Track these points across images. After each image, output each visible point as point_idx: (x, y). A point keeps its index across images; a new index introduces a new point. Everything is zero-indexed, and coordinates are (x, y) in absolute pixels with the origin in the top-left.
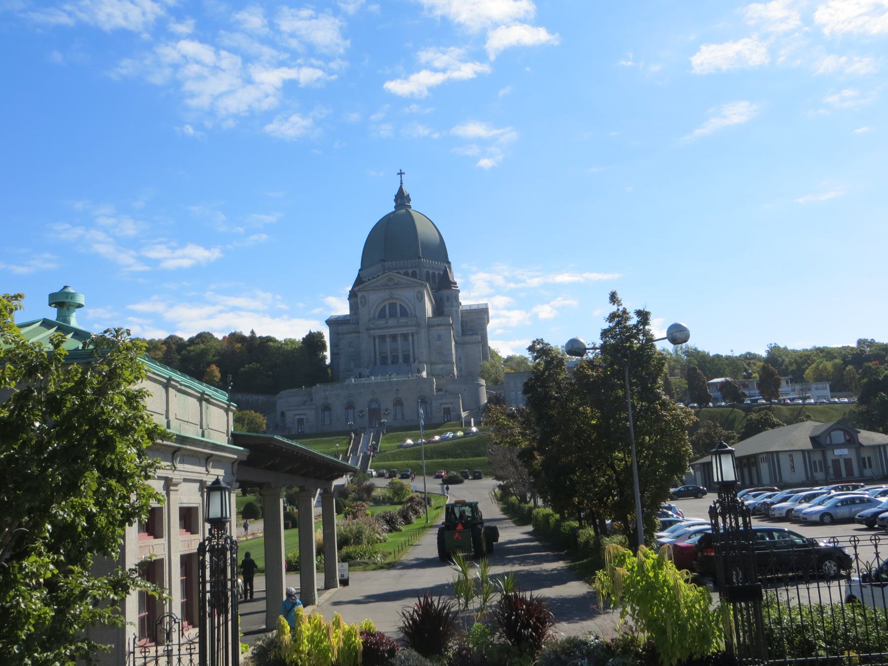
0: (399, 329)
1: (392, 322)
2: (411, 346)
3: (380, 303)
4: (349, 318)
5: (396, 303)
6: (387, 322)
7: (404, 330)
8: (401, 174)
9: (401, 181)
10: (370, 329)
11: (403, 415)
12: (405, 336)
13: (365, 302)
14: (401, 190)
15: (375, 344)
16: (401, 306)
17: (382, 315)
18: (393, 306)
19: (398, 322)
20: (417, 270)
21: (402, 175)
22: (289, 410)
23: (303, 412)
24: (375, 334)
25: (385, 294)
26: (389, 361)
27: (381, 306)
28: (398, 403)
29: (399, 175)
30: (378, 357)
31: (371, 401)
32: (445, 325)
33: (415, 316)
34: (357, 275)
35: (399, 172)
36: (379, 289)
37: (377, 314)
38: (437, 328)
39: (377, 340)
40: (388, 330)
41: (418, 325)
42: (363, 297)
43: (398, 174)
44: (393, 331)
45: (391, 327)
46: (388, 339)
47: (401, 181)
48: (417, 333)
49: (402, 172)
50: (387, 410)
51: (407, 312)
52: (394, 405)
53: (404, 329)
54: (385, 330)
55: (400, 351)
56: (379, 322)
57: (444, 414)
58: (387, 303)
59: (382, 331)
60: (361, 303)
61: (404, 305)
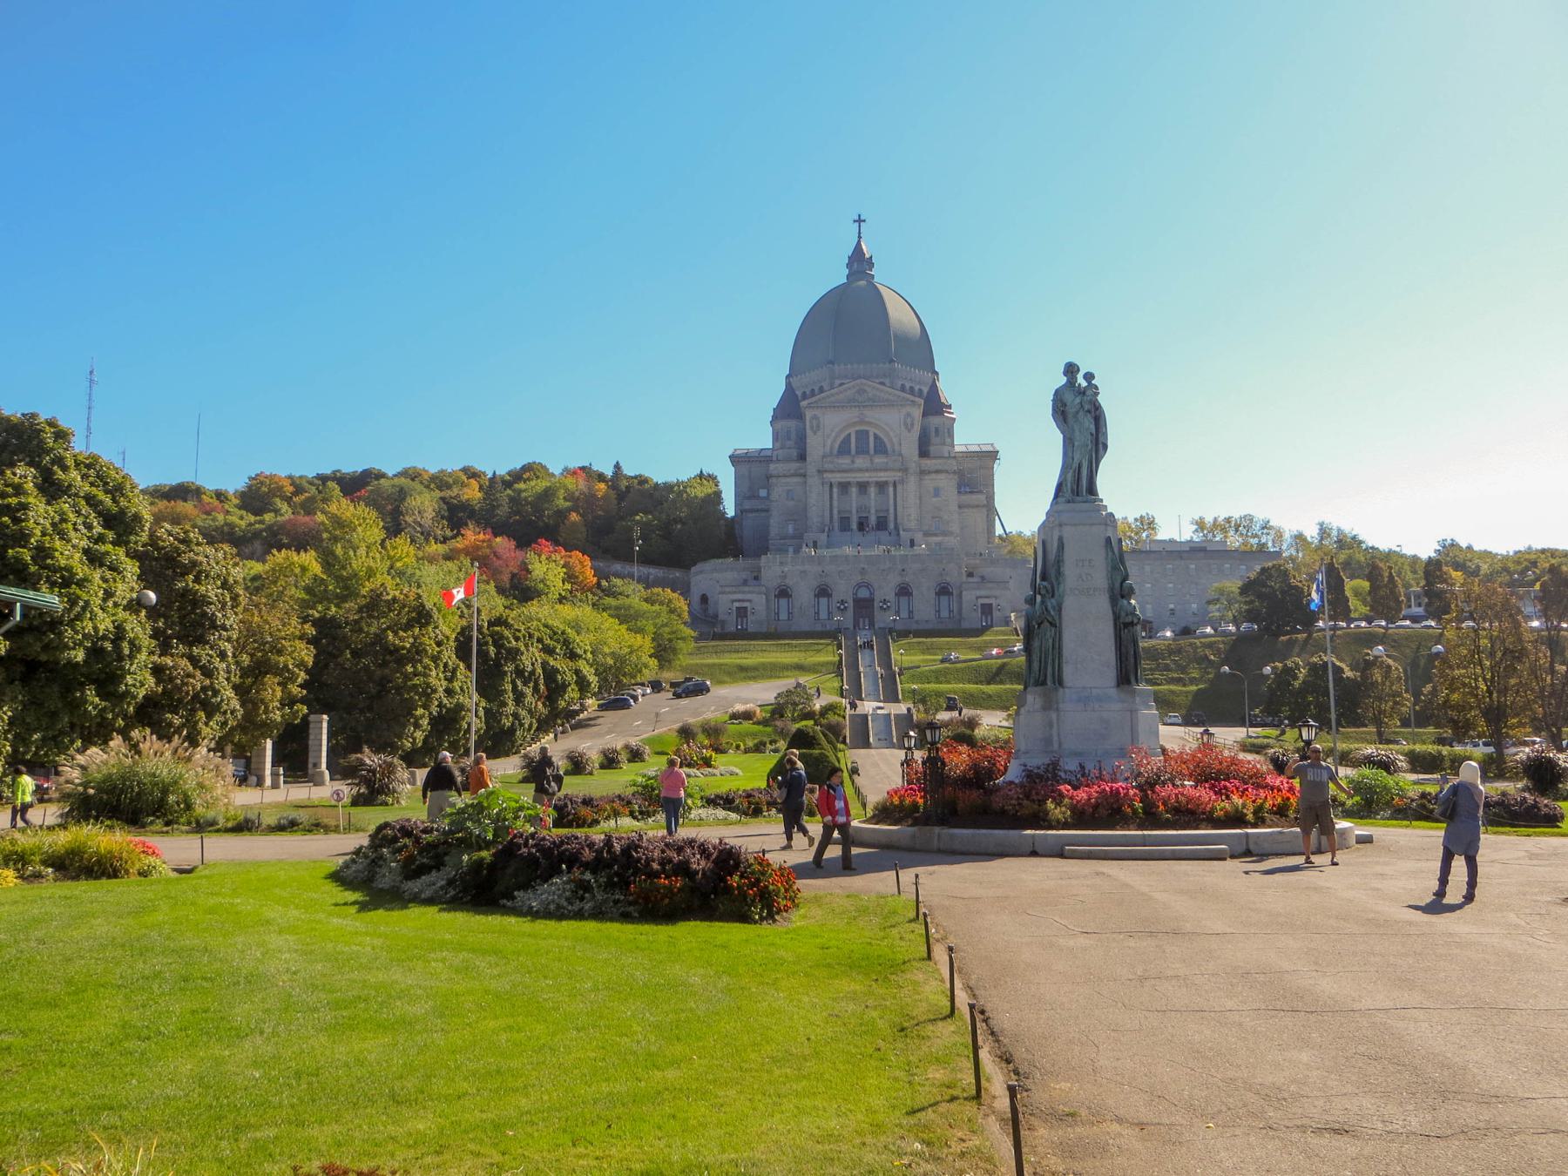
1: (861, 462)
2: (891, 501)
3: (841, 431)
4: (769, 453)
5: (867, 432)
6: (853, 462)
7: (883, 476)
8: (860, 221)
9: (859, 233)
10: (826, 471)
11: (910, 612)
12: (882, 486)
13: (818, 426)
14: (858, 249)
15: (831, 497)
16: (876, 437)
17: (844, 449)
18: (862, 435)
19: (872, 463)
20: (887, 381)
22: (723, 593)
23: (748, 596)
24: (833, 480)
26: (854, 526)
27: (842, 436)
28: (904, 591)
29: (857, 224)
30: (836, 516)
31: (859, 586)
32: (947, 472)
33: (900, 455)
34: (781, 388)
35: (857, 218)
37: (837, 446)
38: (933, 476)
39: (835, 490)
40: (853, 475)
41: (905, 470)
42: (815, 417)
45: (860, 470)
47: (859, 233)
48: (902, 481)
49: (862, 218)
50: (885, 602)
51: (885, 446)
52: (896, 594)
53: (882, 474)
55: (873, 511)
56: (840, 461)
57: (983, 613)
58: (852, 431)
59: (845, 475)
60: (812, 427)
61: (881, 435)
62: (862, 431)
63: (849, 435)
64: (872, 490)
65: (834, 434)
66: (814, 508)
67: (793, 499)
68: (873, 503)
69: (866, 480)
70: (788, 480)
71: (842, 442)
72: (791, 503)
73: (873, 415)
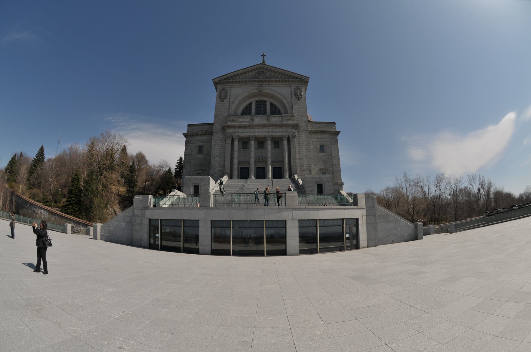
0: (270, 130)
5: (265, 102)
6: (252, 120)
7: (278, 132)
8: (263, 56)
13: (226, 96)
19: (269, 121)
21: (265, 57)
24: (234, 135)
25: (251, 89)
27: (245, 104)
29: (262, 57)
30: (236, 166)
35: (262, 55)
36: (246, 82)
37: (240, 111)
38: (319, 136)
39: (236, 143)
42: (224, 90)
43: (262, 56)
44: (261, 133)
46: (253, 143)
54: (248, 130)
55: (269, 161)
56: (242, 120)
58: (253, 101)
61: (277, 104)
62: (261, 101)
63: (251, 103)
64: (269, 145)
65: (238, 101)
66: (217, 159)
67: (203, 154)
68: (269, 154)
69: (264, 134)
70: (200, 138)
71: (246, 108)
72: (200, 156)
73: (268, 89)
